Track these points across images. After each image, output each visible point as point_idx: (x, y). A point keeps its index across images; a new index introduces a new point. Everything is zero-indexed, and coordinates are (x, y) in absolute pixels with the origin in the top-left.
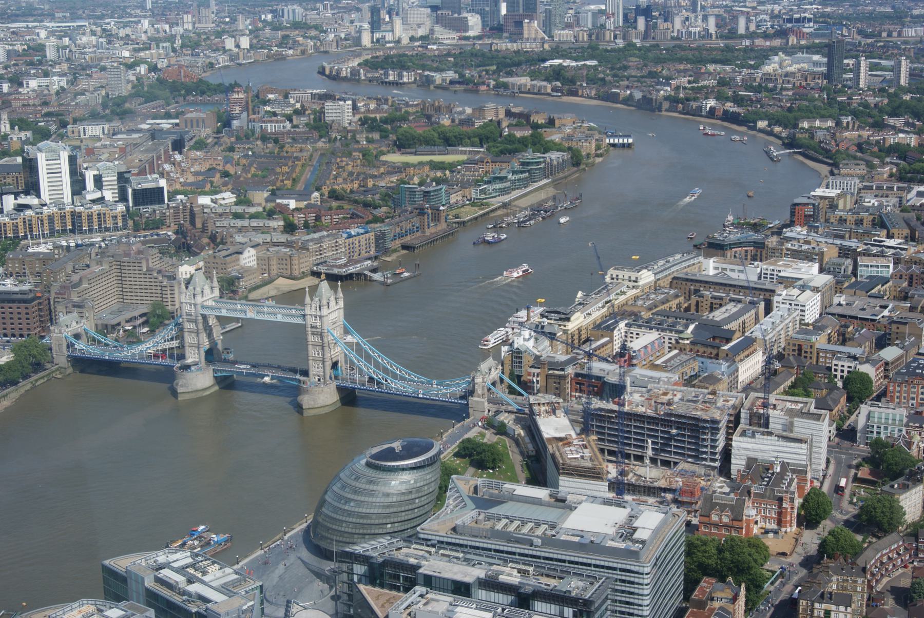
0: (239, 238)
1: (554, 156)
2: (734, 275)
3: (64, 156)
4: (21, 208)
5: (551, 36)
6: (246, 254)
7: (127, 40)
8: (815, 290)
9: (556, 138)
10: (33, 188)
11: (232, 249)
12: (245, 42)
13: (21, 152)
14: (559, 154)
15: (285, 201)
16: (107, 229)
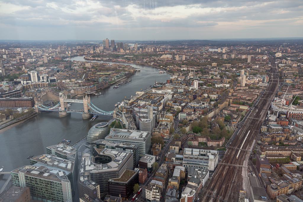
0: (70, 88)
1: (126, 72)
2: (158, 92)
3: (36, 74)
4: (27, 83)
5: (125, 51)
6: (72, 91)
7: (47, 53)
8: (171, 94)
9: (126, 69)
10: (30, 80)
11: (69, 90)
12: (70, 52)
13: (27, 73)
14: (127, 72)
15: (79, 81)
16: (45, 87)
